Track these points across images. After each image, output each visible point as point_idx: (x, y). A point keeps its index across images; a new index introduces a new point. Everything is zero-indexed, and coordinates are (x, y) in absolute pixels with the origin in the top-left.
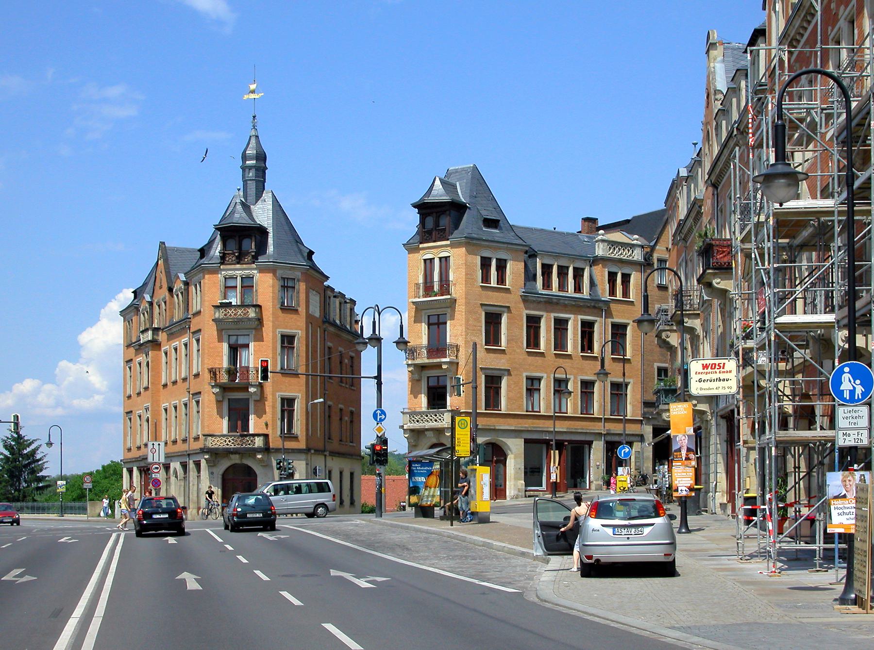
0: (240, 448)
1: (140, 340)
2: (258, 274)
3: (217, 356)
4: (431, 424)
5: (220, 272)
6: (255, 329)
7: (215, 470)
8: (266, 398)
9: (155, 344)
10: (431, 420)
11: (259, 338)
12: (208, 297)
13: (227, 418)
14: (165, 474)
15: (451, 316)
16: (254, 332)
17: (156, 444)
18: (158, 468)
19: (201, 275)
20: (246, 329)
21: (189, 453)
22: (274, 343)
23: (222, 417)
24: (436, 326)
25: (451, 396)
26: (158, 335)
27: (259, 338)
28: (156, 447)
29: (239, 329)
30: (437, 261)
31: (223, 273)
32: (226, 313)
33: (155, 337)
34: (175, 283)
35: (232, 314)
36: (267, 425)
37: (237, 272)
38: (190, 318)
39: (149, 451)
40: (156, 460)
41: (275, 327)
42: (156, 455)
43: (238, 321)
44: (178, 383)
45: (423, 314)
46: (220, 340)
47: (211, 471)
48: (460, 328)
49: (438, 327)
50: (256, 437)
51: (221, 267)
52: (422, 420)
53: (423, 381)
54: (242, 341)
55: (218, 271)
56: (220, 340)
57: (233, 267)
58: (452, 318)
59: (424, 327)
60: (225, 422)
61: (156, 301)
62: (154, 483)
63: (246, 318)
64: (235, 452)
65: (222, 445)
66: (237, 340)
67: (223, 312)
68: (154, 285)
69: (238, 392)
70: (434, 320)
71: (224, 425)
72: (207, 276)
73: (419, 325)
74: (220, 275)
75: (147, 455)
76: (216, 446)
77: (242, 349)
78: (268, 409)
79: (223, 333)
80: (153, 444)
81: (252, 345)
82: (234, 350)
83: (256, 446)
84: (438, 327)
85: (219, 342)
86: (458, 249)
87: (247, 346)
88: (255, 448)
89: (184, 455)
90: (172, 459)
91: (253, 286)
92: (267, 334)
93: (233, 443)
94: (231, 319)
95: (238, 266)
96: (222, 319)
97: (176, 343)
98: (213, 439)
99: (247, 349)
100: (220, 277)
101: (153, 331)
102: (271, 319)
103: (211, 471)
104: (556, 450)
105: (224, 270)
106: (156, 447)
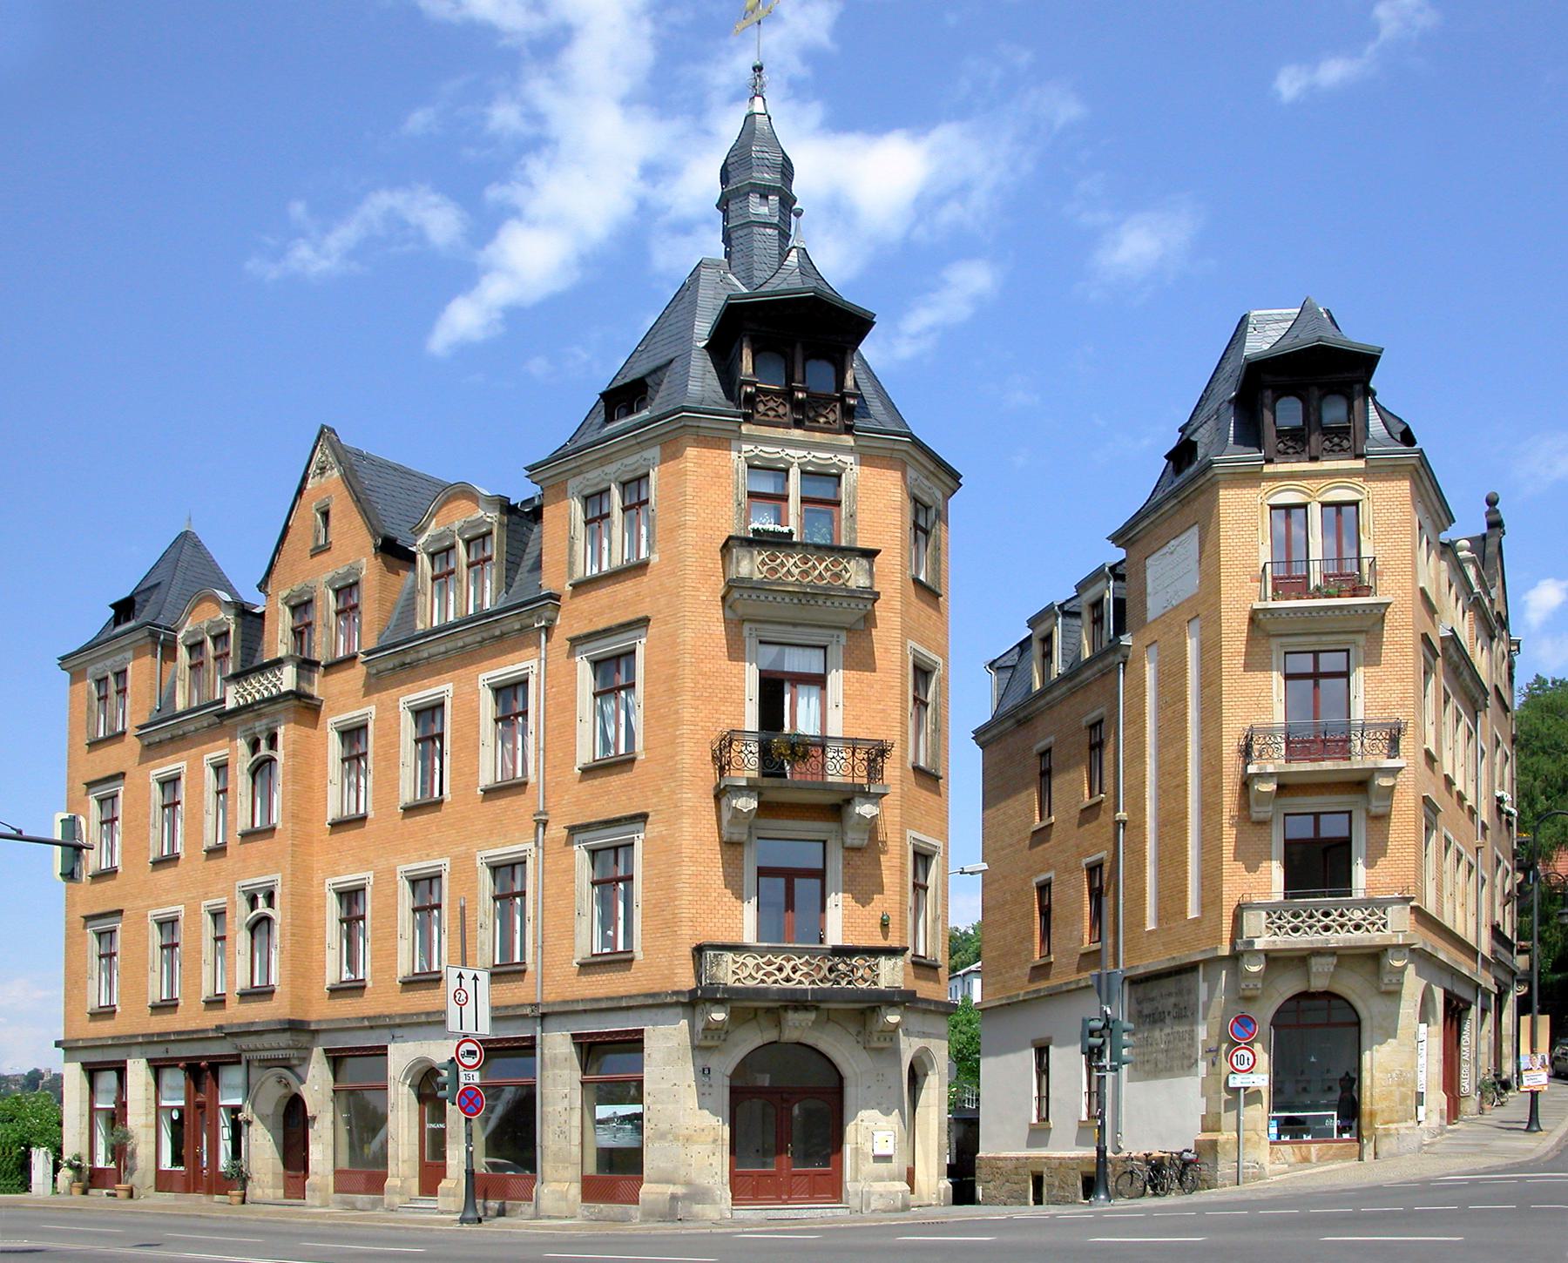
0: (830, 989)
1: (223, 701)
2: (857, 468)
3: (724, 700)
4: (1343, 935)
5: (734, 444)
6: (848, 630)
7: (714, 1061)
8: (884, 843)
9: (305, 706)
10: (1342, 926)
11: (862, 660)
12: (697, 514)
13: (754, 901)
14: (331, 1077)
15: (1366, 655)
16: (843, 640)
17: (468, 974)
18: (474, 1053)
19: (655, 452)
20: (820, 627)
21: (545, 1011)
22: (904, 676)
23: (740, 896)
24: (1311, 682)
25: (1370, 864)
26: (311, 682)
27: (862, 660)
28: (468, 984)
29: (795, 625)
30: (1315, 511)
31: (745, 447)
32: (773, 564)
33: (306, 687)
34: (433, 515)
35: (796, 571)
36: (884, 925)
37: (792, 452)
38: (558, 598)
39: (451, 996)
40: (469, 1028)
41: (907, 632)
42: (469, 1010)
43: (808, 596)
44: (119, 875)
45: (1274, 647)
46: (736, 652)
47: (700, 1063)
48: (1399, 686)
49: (1316, 685)
50: (882, 960)
51: (745, 429)
52: (1310, 927)
53: (1274, 827)
54: (797, 661)
55: (729, 440)
56: (736, 652)
57: (779, 433)
58: (1373, 659)
59: (1277, 678)
60: (749, 910)
61: (284, 593)
62: (465, 1102)
63: (838, 588)
64: (796, 1002)
65: (770, 980)
66: (781, 657)
67: (763, 563)
68: (278, 550)
69: (794, 818)
70: (1305, 664)
71: (746, 923)
72: (691, 452)
73: (1260, 675)
74: (734, 454)
75: (444, 1012)
76: (750, 983)
77: (802, 689)
78: (889, 878)
79: (746, 633)
80: (460, 976)
81: (836, 679)
82: (772, 691)
83: (882, 985)
84: (1316, 685)
85: (731, 658)
86: (1387, 484)
87: (819, 681)
88: (880, 993)
89: (525, 1016)
90: (398, 1032)
91: (838, 504)
92: (887, 650)
93: (807, 974)
94: (792, 584)
95: (797, 434)
96: (761, 581)
97: (441, 688)
98: (740, 959)
99: (815, 690)
100: (735, 459)
101: (298, 667)
102: (898, 605)
103: (700, 1063)
104: (1542, 1012)
105: (750, 439)
106: (468, 984)
